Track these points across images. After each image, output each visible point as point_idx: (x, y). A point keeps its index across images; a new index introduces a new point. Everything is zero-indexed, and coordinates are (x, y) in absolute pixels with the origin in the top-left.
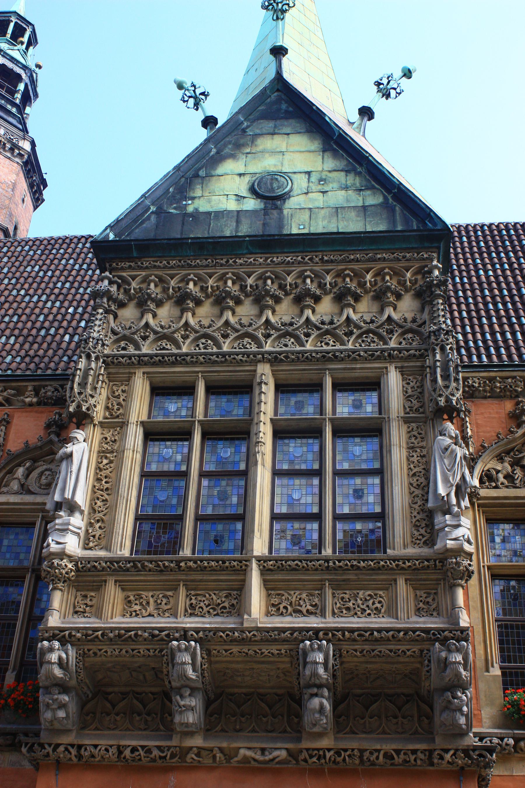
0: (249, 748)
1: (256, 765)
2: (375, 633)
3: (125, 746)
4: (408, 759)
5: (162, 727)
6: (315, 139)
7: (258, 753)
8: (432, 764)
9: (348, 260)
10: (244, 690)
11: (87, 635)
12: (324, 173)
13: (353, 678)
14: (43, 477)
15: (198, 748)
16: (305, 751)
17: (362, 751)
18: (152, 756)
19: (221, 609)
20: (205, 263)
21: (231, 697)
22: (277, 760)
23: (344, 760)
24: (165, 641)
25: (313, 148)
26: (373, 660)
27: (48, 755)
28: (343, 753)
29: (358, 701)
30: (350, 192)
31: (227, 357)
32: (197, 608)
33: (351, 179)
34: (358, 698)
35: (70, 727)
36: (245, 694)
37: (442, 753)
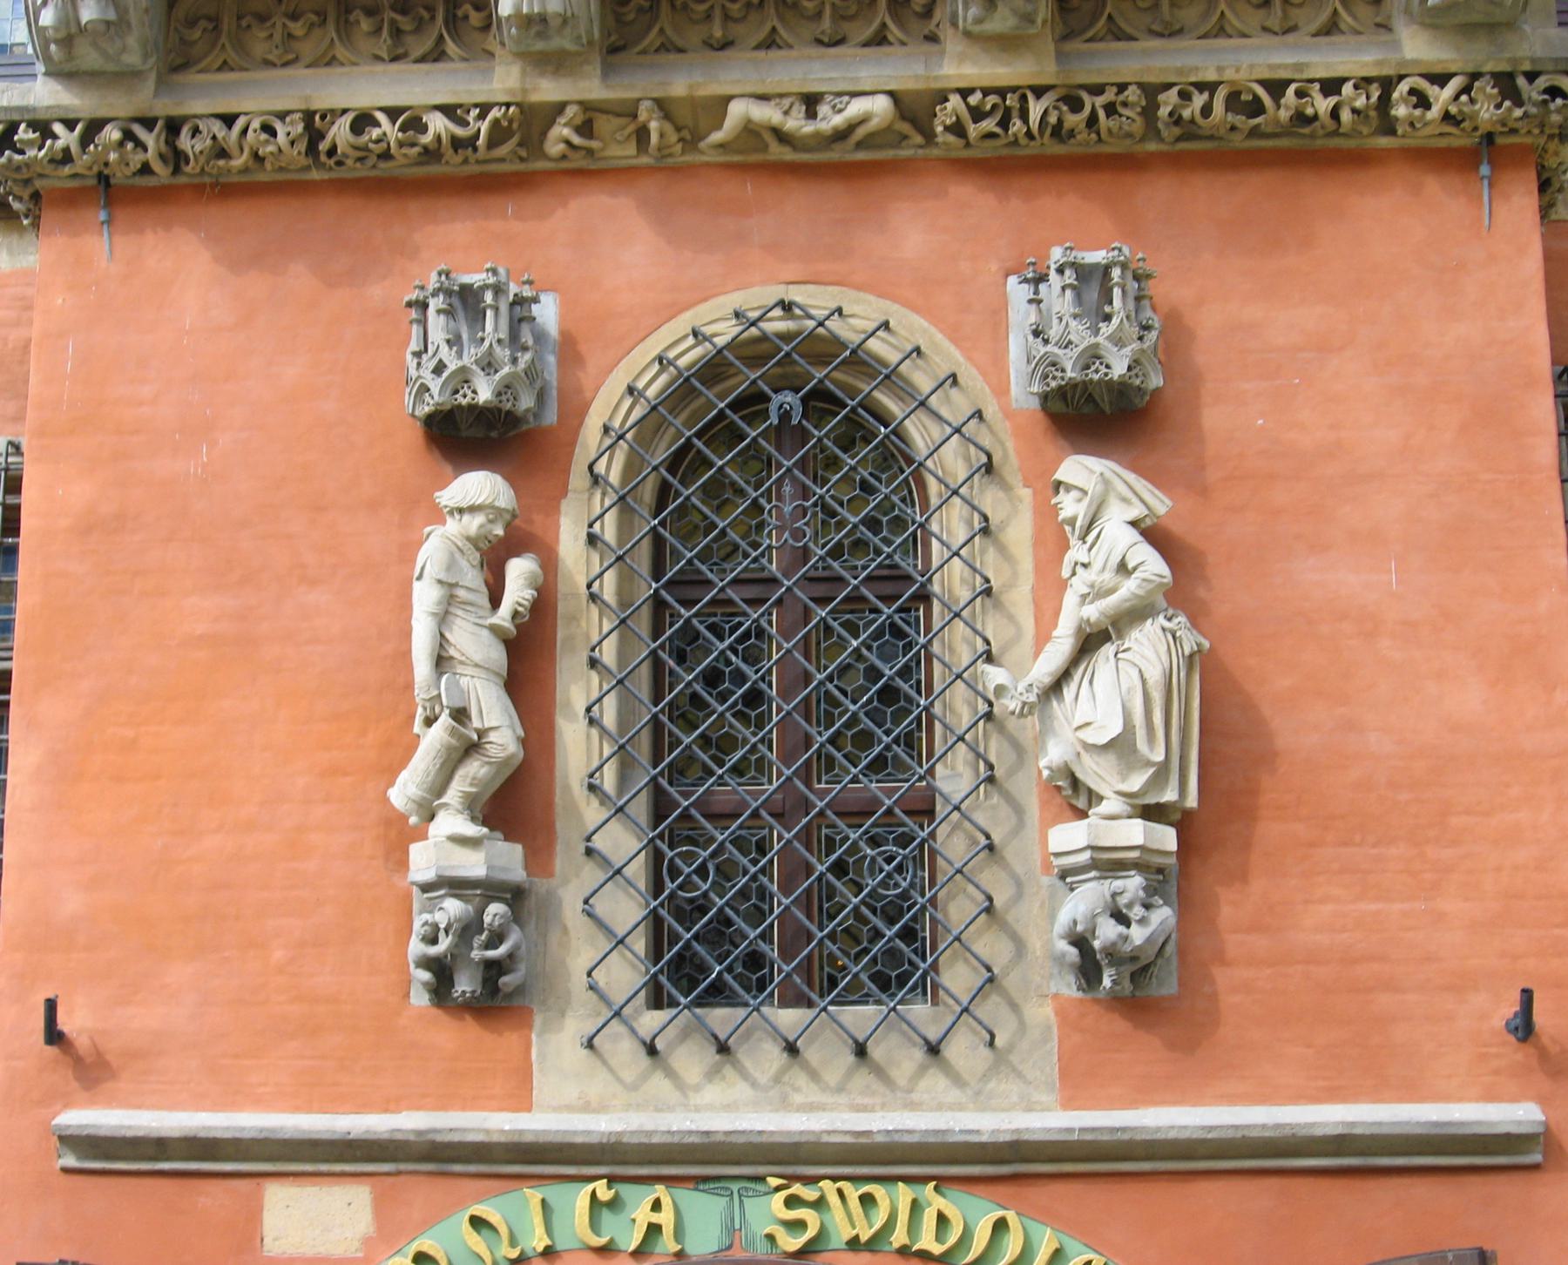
0: (763, 98)
1: (788, 155)
3: (332, 111)
4: (1309, 111)
7: (794, 112)
8: (1388, 126)
15: (586, 106)
16: (955, 101)
17: (1152, 92)
18: (427, 139)
22: (860, 132)
23: (1092, 121)
27: (66, 157)
28: (1087, 99)
35: (133, 59)
37: (1423, 84)
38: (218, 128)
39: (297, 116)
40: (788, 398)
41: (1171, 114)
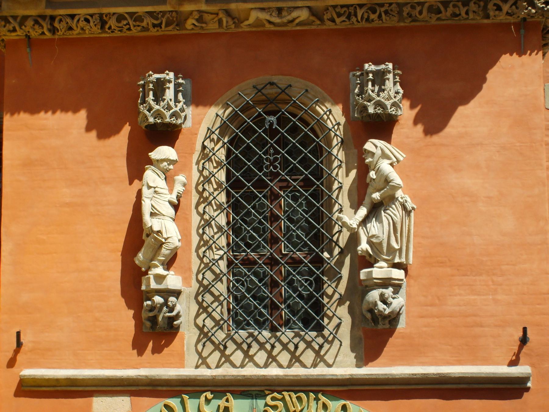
0: (262, 9)
1: (272, 28)
15: (200, 11)
22: (297, 21)
23: (380, 17)
38: (69, 20)
39: (97, 16)
40: (273, 119)
41: (408, 14)
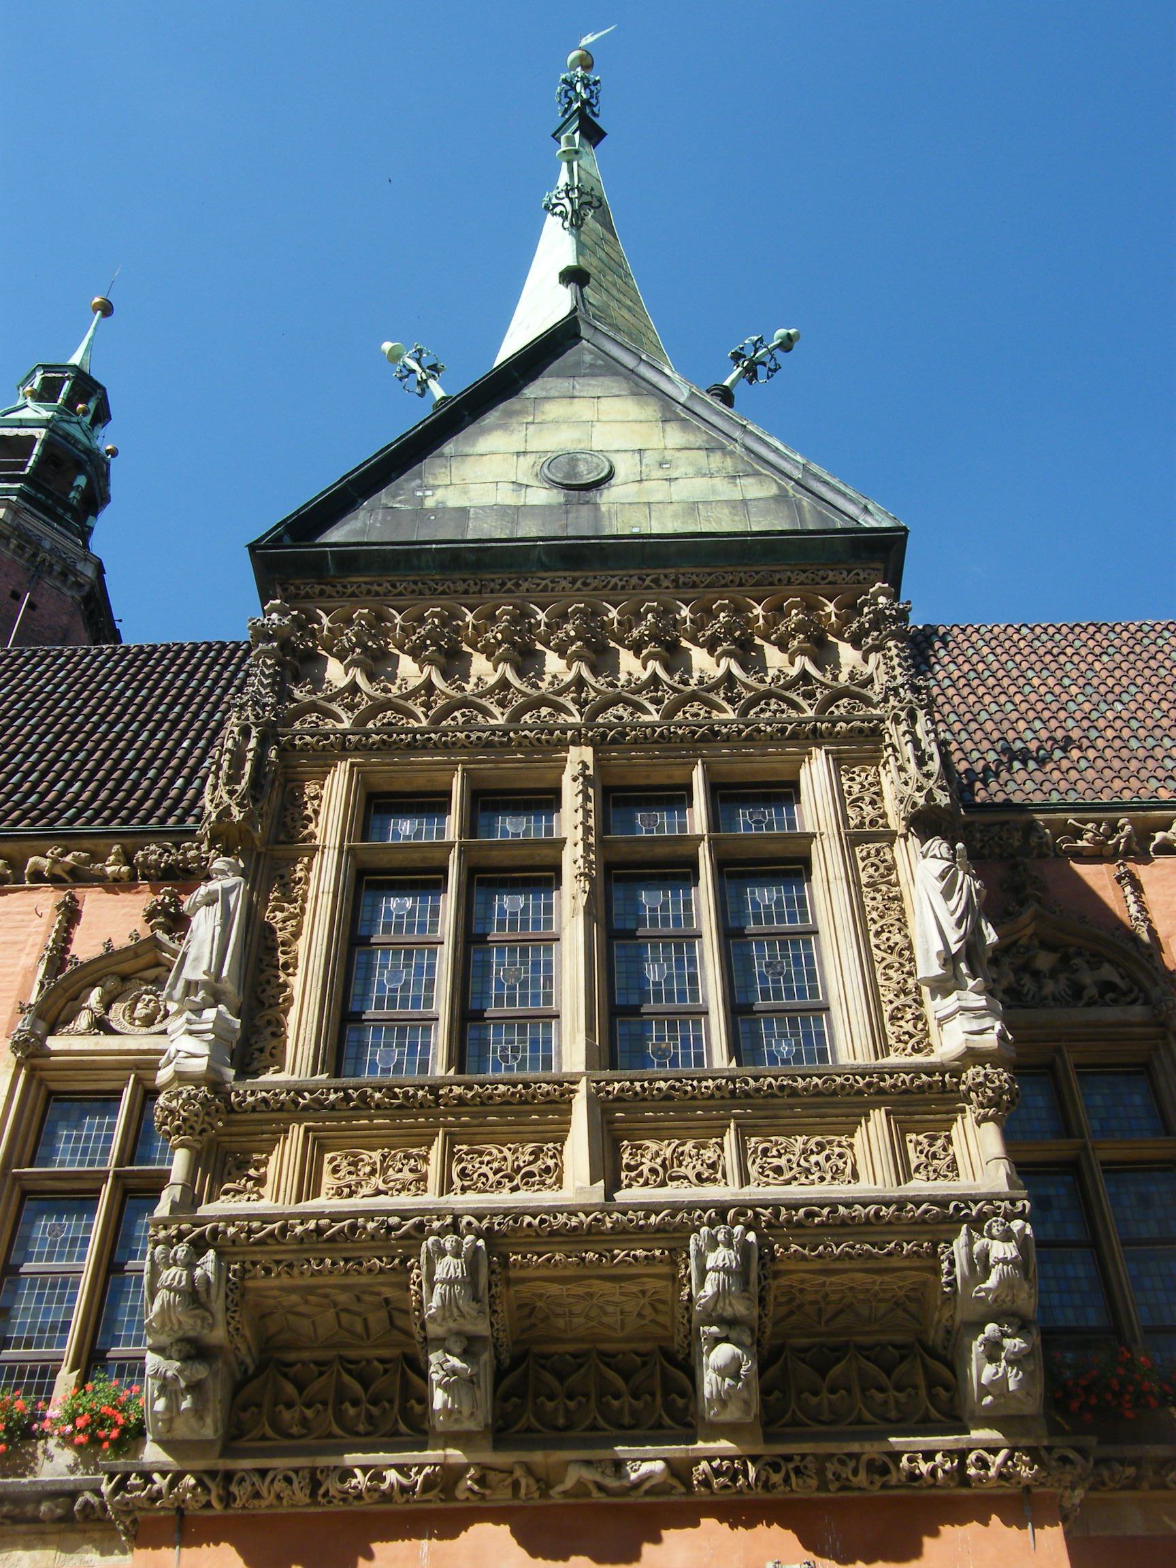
0: (588, 1463)
2: (842, 1209)
3: (328, 1468)
5: (403, 1428)
6: (647, 404)
9: (723, 582)
10: (570, 1348)
11: (250, 1232)
12: (667, 453)
13: (791, 1313)
14: (140, 1005)
18: (384, 1486)
19: (522, 1179)
20: (461, 586)
21: (543, 1361)
23: (787, 1480)
24: (415, 1238)
25: (642, 417)
26: (838, 1265)
29: (803, 1360)
30: (717, 481)
31: (512, 734)
32: (475, 1176)
33: (716, 460)
34: (803, 1355)
36: (574, 1356)
38: (256, 1479)
